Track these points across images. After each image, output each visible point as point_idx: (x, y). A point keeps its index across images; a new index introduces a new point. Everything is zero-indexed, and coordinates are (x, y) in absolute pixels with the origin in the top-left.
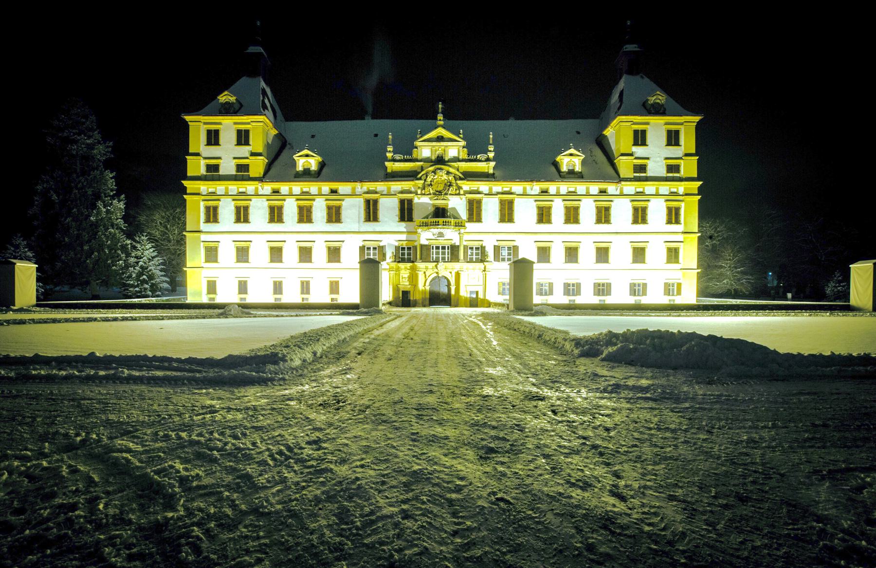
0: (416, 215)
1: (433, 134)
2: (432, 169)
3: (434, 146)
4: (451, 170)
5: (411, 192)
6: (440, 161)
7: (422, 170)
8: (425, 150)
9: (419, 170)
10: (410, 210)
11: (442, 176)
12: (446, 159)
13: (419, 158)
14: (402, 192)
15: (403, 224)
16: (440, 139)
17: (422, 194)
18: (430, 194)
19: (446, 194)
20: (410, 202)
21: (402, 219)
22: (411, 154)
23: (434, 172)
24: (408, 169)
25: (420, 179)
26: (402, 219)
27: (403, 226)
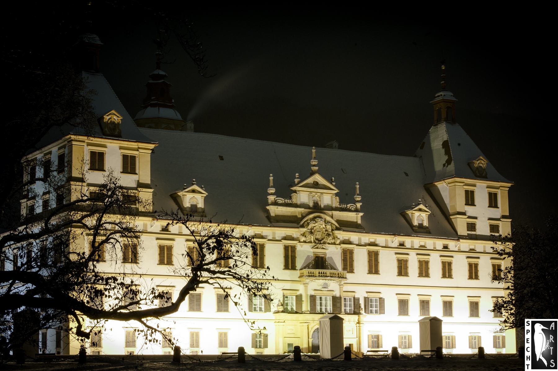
0: (299, 263)
1: (310, 180)
2: (311, 216)
3: (311, 192)
4: (328, 219)
5: (292, 239)
6: (317, 208)
7: (303, 217)
8: (303, 196)
9: (300, 216)
10: (294, 258)
11: (319, 225)
12: (322, 206)
13: (299, 203)
14: (285, 238)
15: (288, 272)
16: (316, 185)
17: (305, 242)
18: (310, 242)
19: (324, 243)
20: (293, 248)
21: (286, 267)
22: (290, 198)
23: (314, 219)
24: (289, 214)
25: (302, 226)
26: (286, 267)
27: (289, 274)
